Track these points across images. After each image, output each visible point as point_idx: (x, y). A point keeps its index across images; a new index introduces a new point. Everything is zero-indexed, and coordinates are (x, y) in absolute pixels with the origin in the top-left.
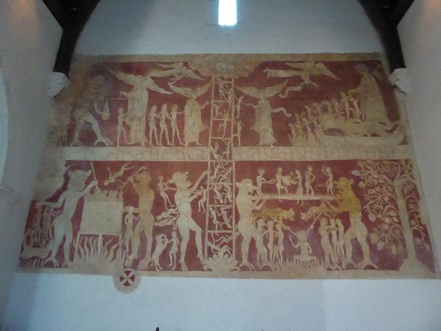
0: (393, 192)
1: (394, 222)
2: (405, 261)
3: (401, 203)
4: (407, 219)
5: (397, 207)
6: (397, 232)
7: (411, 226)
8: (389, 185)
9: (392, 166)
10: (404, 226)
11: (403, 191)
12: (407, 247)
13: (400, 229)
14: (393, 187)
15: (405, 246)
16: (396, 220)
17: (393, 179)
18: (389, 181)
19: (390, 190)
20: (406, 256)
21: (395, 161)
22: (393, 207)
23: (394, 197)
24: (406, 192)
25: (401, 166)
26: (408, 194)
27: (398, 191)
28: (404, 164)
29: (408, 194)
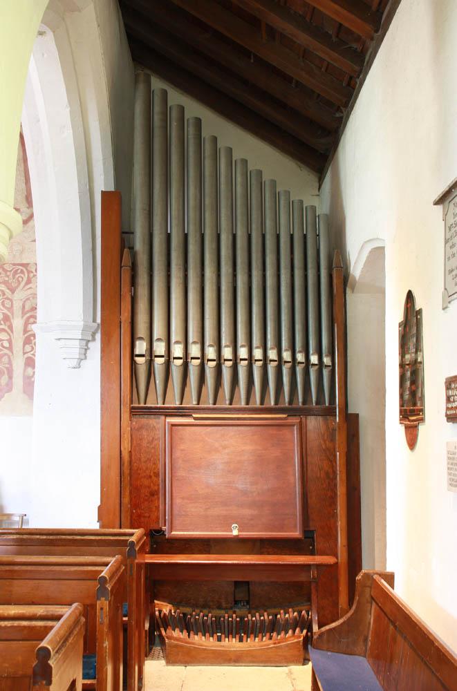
0: (11, 309)
1: (4, 347)
2: (6, 395)
3: (18, 323)
4: (21, 344)
5: (11, 327)
6: (5, 359)
7: (24, 353)
8: (8, 299)
9: (16, 272)
10: (14, 352)
11: (24, 307)
12: (14, 380)
13: (9, 357)
14: (11, 300)
15: (11, 378)
16: (6, 344)
17: (13, 291)
18: (8, 292)
19: (8, 306)
20: (10, 390)
21: (22, 265)
22: (6, 328)
23: (9, 314)
24: (27, 307)
25: (29, 272)
26: (28, 311)
27: (17, 306)
28: (34, 271)
29: (28, 311)
